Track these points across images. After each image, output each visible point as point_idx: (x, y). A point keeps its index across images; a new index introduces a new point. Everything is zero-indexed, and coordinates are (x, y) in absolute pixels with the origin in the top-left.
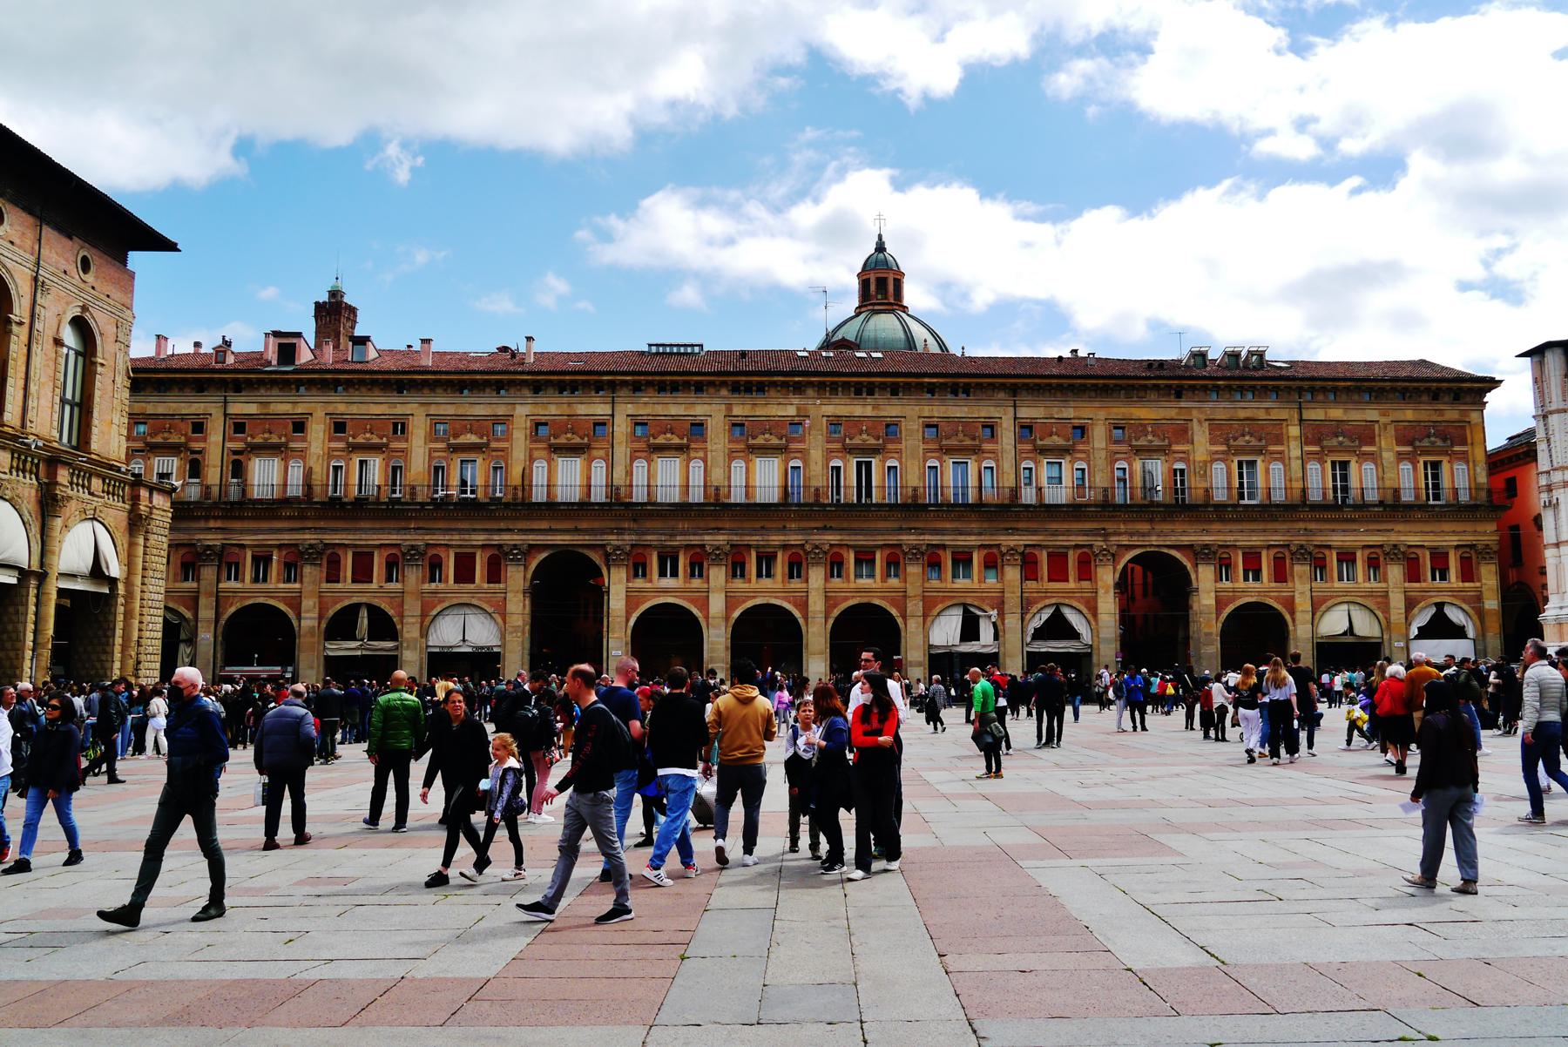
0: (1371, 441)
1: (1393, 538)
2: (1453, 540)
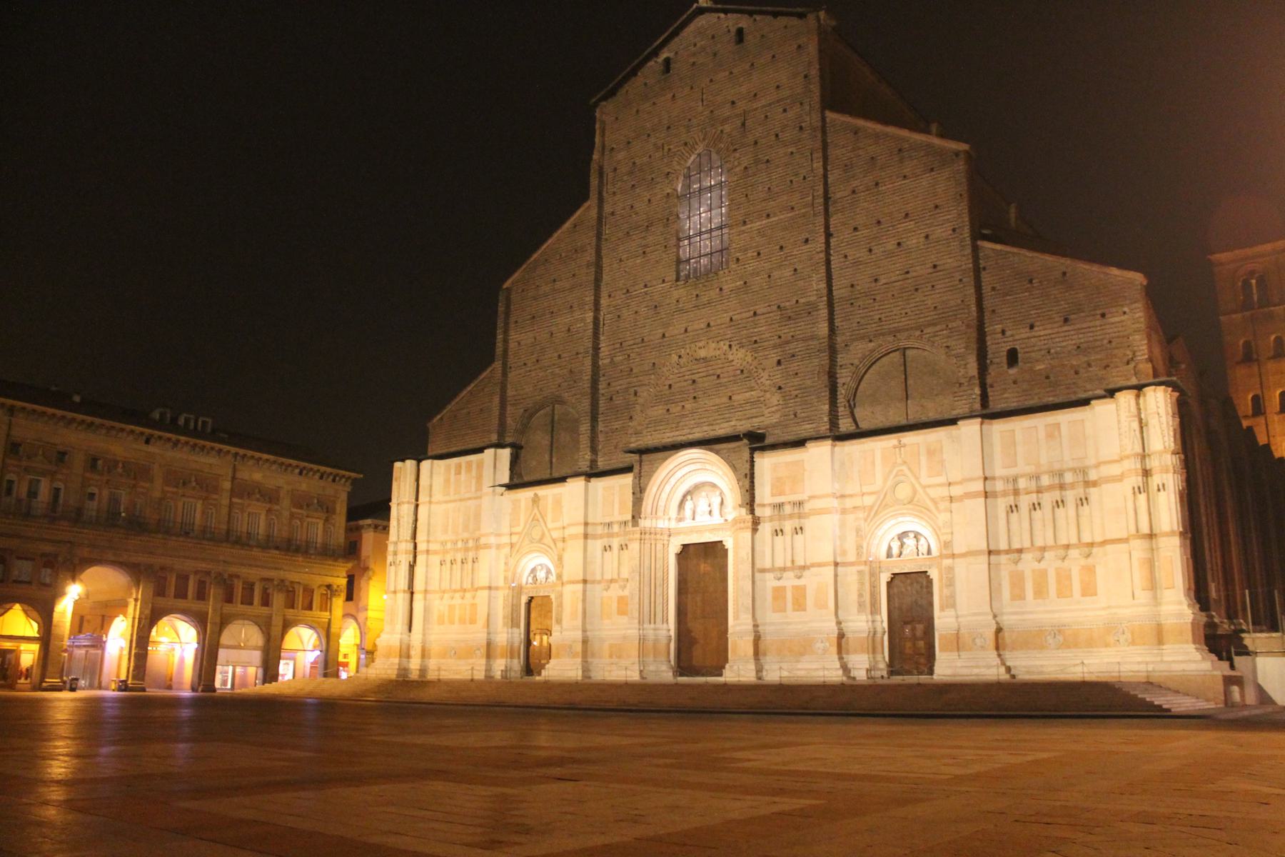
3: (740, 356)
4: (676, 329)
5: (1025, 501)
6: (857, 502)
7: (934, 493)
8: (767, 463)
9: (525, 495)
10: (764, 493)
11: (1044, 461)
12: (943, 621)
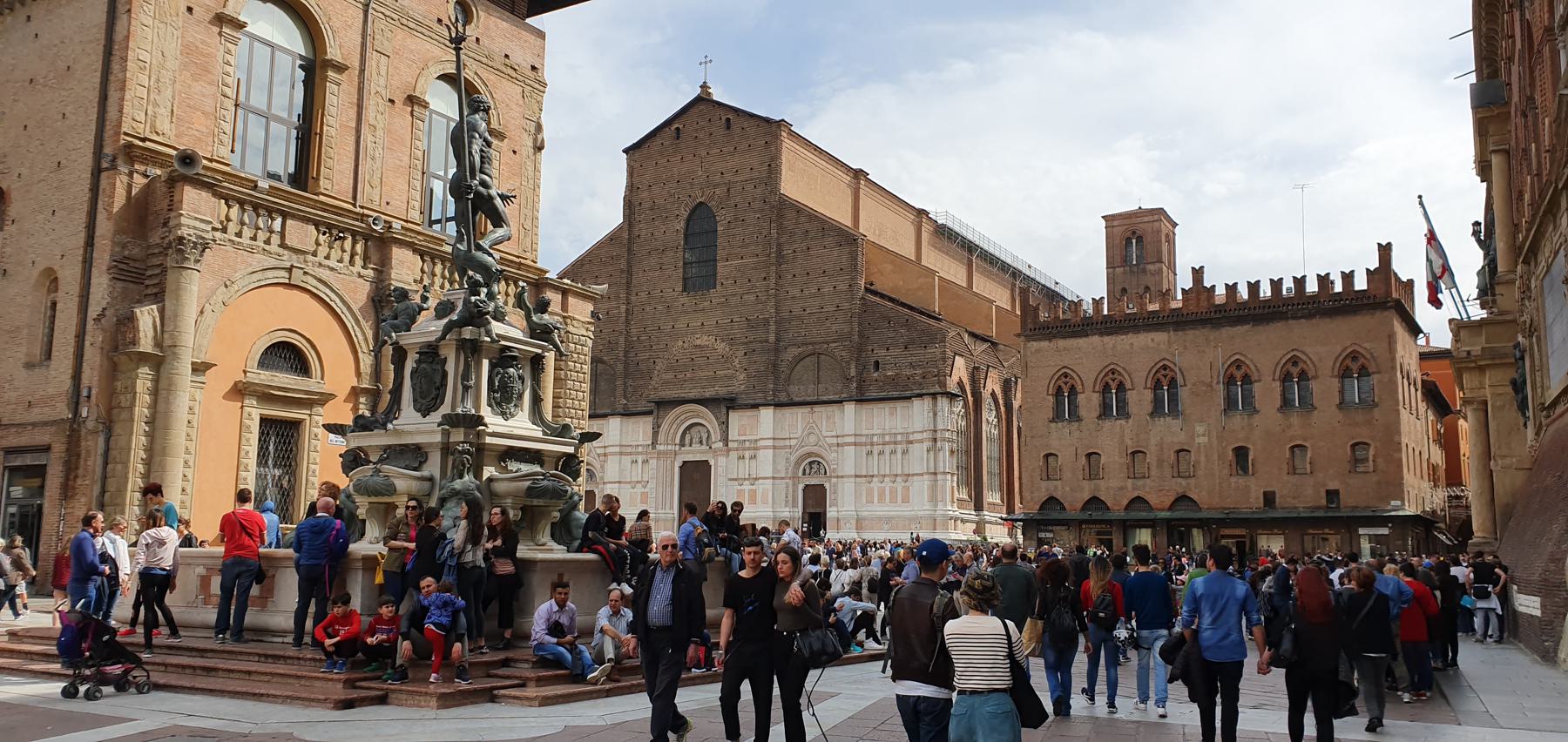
3: (722, 347)
4: (681, 325)
5: (876, 450)
6: (787, 443)
7: (830, 441)
8: (734, 417)
10: (733, 434)
12: (831, 513)
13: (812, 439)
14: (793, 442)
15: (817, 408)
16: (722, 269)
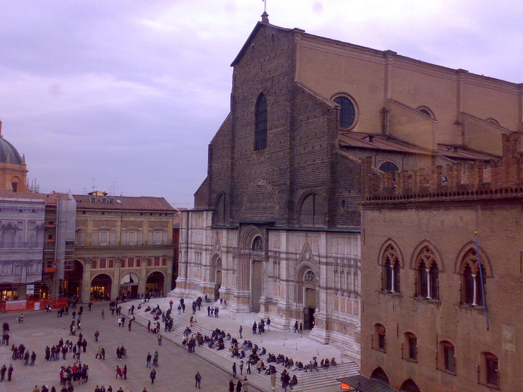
0: (142, 227)
1: (145, 255)
2: (161, 254)
3: (269, 187)
5: (340, 269)
6: (294, 256)
8: (272, 236)
9: (215, 231)
11: (346, 253)
13: (308, 256)
14: (298, 256)
15: (309, 234)
16: (270, 134)
